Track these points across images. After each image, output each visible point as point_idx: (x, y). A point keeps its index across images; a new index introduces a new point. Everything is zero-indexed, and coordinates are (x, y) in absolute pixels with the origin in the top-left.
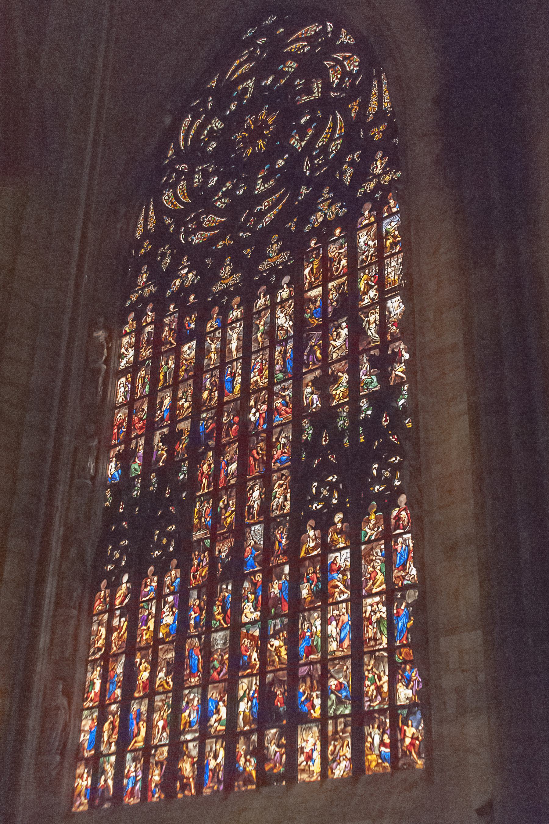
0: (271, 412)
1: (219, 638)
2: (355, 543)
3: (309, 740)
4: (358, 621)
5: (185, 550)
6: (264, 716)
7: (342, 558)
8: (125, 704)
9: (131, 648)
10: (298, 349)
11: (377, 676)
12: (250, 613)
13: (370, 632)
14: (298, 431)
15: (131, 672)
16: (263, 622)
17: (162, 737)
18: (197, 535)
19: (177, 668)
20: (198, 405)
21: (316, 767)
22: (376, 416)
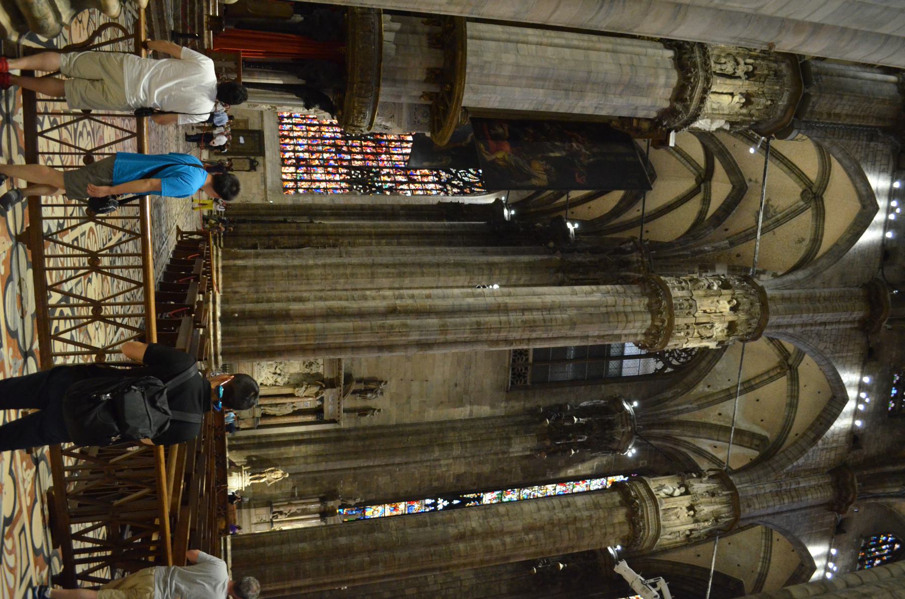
0: (383, 161)
1: (320, 148)
2: (341, 181)
3: (292, 169)
4: (320, 181)
5: (346, 139)
6: (298, 159)
7: (337, 178)
8: (306, 124)
9: (321, 125)
10: (402, 169)
11: (305, 185)
12: (326, 156)
13: (317, 184)
14: (376, 168)
15: (314, 125)
16: (323, 159)
17: (296, 134)
18: (350, 142)
19: (314, 138)
20: (391, 141)
21: (285, 171)
22: (375, 187)
